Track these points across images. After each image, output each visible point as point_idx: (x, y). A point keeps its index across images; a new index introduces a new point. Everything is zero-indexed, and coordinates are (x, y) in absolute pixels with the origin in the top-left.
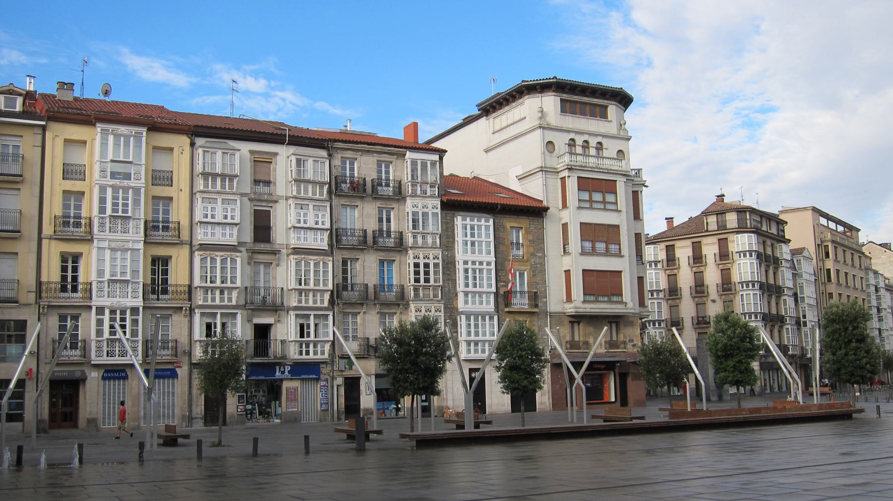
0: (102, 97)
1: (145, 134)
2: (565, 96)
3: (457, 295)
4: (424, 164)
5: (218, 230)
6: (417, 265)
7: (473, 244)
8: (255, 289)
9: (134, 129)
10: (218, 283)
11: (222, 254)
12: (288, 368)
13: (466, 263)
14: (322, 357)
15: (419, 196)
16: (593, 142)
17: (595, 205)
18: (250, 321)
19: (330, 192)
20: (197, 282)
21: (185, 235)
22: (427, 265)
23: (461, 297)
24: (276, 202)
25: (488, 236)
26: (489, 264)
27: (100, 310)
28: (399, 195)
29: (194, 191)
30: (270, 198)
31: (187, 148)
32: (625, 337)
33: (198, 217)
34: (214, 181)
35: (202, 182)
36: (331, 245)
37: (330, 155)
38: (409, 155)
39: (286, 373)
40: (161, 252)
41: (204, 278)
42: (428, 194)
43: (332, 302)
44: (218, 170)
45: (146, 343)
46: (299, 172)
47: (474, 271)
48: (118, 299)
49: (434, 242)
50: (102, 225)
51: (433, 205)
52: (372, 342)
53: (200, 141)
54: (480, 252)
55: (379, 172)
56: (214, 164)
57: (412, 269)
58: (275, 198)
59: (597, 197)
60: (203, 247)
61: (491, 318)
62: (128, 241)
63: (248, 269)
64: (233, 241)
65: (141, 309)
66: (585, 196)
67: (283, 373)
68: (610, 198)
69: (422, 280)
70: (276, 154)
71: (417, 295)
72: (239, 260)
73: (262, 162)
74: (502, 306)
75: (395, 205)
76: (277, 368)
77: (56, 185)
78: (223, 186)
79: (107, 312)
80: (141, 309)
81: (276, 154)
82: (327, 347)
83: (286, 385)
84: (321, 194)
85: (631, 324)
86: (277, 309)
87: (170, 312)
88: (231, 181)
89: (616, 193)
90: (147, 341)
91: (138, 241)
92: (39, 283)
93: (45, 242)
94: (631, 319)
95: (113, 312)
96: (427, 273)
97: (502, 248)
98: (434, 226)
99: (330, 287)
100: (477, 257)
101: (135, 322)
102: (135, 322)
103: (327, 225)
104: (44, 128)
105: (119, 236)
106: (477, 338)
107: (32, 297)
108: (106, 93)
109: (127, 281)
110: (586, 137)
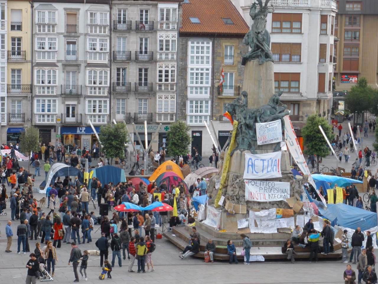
1: (6, 4)
3: (186, 88)
4: (168, 11)
6: (161, 71)
7: (197, 57)
8: (68, 86)
12: (84, 129)
13: (192, 69)
14: (103, 123)
15: (165, 30)
17: (284, 31)
18: (63, 103)
19: (110, 30)
20: (35, 83)
21: (29, 58)
22: (167, 72)
23: (189, 90)
24: (79, 37)
25: (208, 52)
26: (207, 69)
28: (153, 29)
29: (34, 33)
31: (30, 9)
32: (303, 113)
33: (36, 48)
34: (44, 27)
35: (37, 28)
36: (110, 61)
37: (111, 8)
39: (83, 131)
40: (17, 67)
42: (171, 28)
43: (110, 93)
44: (47, 21)
45: (9, 114)
46: (91, 20)
47: (197, 74)
49: (172, 58)
51: (172, 36)
52: (132, 115)
54: (202, 62)
55: (142, 15)
56: (44, 19)
57: (158, 74)
58: (78, 35)
59: (286, 25)
60: (39, 64)
61: (207, 102)
63: (63, 75)
65: (6, 98)
66: (278, 25)
67: (81, 131)
68: (296, 25)
69: (163, 80)
70: (79, 9)
71: (160, 89)
72: (57, 71)
73: (72, 14)
74: (216, 94)
75: (149, 35)
76: (78, 128)
78: (49, 31)
80: (6, 98)
81: (79, 9)
82: (106, 118)
83: (83, 137)
84: (105, 32)
85: (309, 105)
86: (78, 96)
87: (21, 99)
88: (53, 26)
89: (301, 22)
90: (9, 114)
94: (308, 102)
96: (167, 76)
97: (218, 59)
98: (174, 48)
99: (108, 85)
100: (200, 66)
103: (108, 50)
106: (197, 114)
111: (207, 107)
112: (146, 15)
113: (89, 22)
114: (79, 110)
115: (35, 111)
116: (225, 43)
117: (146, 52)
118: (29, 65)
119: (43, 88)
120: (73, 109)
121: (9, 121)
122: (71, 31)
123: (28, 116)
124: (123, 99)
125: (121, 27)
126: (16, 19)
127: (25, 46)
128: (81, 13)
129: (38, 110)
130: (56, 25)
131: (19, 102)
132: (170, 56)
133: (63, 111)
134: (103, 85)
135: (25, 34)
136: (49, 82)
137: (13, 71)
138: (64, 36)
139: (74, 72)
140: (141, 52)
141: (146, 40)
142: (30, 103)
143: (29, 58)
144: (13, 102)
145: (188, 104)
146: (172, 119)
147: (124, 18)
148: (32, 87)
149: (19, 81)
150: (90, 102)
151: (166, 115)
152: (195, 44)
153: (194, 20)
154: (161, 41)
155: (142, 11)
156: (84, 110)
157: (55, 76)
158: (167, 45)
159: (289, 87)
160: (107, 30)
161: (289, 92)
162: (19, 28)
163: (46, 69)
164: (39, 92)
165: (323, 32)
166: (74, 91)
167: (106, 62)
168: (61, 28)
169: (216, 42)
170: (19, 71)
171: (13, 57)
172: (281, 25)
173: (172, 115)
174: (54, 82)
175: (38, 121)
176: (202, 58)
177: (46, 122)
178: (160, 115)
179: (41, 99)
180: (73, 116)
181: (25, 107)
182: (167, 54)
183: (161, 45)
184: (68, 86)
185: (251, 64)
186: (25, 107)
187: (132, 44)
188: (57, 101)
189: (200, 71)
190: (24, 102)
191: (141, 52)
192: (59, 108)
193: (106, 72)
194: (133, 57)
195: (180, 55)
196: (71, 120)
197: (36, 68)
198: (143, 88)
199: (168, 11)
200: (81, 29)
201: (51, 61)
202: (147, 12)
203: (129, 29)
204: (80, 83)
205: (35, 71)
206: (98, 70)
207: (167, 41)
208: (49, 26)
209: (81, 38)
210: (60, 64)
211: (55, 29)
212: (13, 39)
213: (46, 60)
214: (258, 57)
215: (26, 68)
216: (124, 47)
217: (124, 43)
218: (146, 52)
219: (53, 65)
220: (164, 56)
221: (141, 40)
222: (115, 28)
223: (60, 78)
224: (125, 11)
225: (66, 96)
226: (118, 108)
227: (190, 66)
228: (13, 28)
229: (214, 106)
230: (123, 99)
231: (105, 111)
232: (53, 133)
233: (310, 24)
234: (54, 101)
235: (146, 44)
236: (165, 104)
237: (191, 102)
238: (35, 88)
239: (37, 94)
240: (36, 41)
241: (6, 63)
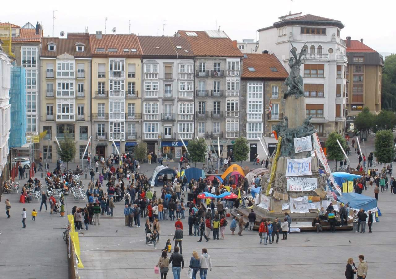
0: (113, 33)
2: (303, 26)
3: (246, 115)
4: (233, 63)
6: (228, 104)
7: (254, 94)
9: (121, 59)
11: (152, 102)
12: (177, 143)
13: (250, 102)
14: (190, 139)
15: (231, 76)
16: (316, 46)
17: (312, 76)
18: (163, 125)
19: (194, 76)
20: (144, 112)
21: (140, 96)
22: (233, 104)
23: (248, 116)
24: (173, 81)
25: (261, 91)
26: (260, 102)
27: (111, 123)
28: (223, 76)
29: (143, 79)
30: (171, 80)
31: (140, 63)
32: (326, 131)
33: (145, 89)
37: (195, 62)
38: (228, 60)
39: (176, 144)
40: (131, 102)
42: (235, 75)
43: (194, 118)
44: (152, 72)
45: (126, 133)
46: (181, 70)
47: (253, 105)
48: (117, 119)
49: (237, 95)
50: (111, 94)
51: (237, 80)
52: (210, 134)
53: (145, 60)
55: (215, 66)
56: (150, 70)
57: (227, 105)
58: (173, 80)
59: (313, 72)
60: (146, 100)
61: (260, 124)
62: (120, 99)
63: (162, 107)
65: (125, 123)
66: (308, 72)
67: (175, 144)
68: (320, 72)
69: (231, 109)
70: (173, 63)
71: (228, 115)
72: (159, 104)
73: (168, 66)
74: (266, 119)
75: (221, 79)
76: (173, 142)
78: (153, 77)
79: (114, 124)
80: (125, 123)
81: (173, 63)
82: (192, 136)
83: (176, 149)
84: (190, 78)
85: (330, 126)
86: (173, 121)
88: (156, 74)
89: (324, 70)
90: (127, 133)
91: (124, 99)
92: (91, 114)
93: (93, 100)
94: (329, 124)
95: (115, 124)
96: (233, 107)
97: (268, 95)
98: (237, 88)
99: (193, 113)
100: (255, 100)
101: (123, 127)
102: (123, 127)
103: (193, 90)
104: (91, 61)
105: (117, 97)
106: (253, 132)
107: (89, 119)
108: (114, 31)
109: (120, 113)
110: (313, 44)
111: (260, 127)
112: (219, 66)
113: (180, 71)
114: (174, 130)
115: (144, 131)
116: (272, 84)
117: (218, 91)
118: (140, 100)
119: (150, 115)
120: (170, 129)
121: (126, 138)
122: (168, 78)
123: (139, 134)
124: (203, 123)
125: (201, 74)
126: (131, 70)
127: (137, 88)
128: (175, 65)
129: (146, 130)
130: (158, 73)
131: (134, 125)
132: (235, 94)
133: (163, 131)
134: (190, 113)
135: (137, 80)
136: (154, 112)
137: (129, 104)
138: (164, 81)
139: (170, 105)
140: (215, 91)
141: (218, 83)
143: (140, 96)
144: (130, 125)
145: (248, 125)
146: (236, 136)
147: (204, 68)
148: (142, 115)
149: (133, 111)
150: (181, 124)
151: (232, 133)
152: (252, 85)
153: (251, 69)
154: (229, 83)
155: (215, 64)
156: (177, 130)
157: (157, 108)
158: (233, 86)
159: (316, 114)
160: (192, 76)
161: (316, 117)
162: (134, 76)
164: (147, 118)
165: (339, 76)
166: (170, 118)
167: (192, 98)
168: (161, 75)
169: (266, 84)
170: (133, 104)
171: (129, 95)
172: (310, 72)
173: (236, 133)
174: (157, 111)
175: (146, 138)
176: (257, 94)
177: (151, 138)
178: (228, 133)
180: (170, 134)
181: (137, 128)
182: (233, 92)
183: (229, 86)
185: (291, 98)
186: (137, 129)
187: (209, 85)
188: (159, 124)
189: (255, 103)
190: (137, 125)
191: (215, 91)
192: (160, 129)
193: (191, 105)
194: (210, 94)
195: (242, 92)
196: (168, 137)
198: (217, 115)
199: (233, 63)
200: (175, 76)
201: (155, 97)
202: (219, 64)
203: (207, 76)
204: (174, 112)
206: (186, 103)
207: (233, 83)
208: (153, 74)
209: (175, 81)
210: (160, 100)
211: (158, 76)
212: (130, 83)
213: (152, 97)
214: (294, 93)
215: (138, 103)
216: (204, 88)
217: (204, 85)
218: (218, 91)
219: (156, 100)
220: (230, 94)
221: (215, 82)
222: (198, 75)
223: (160, 108)
224: (204, 64)
225: (165, 121)
226: (200, 129)
227: (248, 100)
228: (129, 76)
229: (265, 127)
230: (203, 123)
231: (191, 131)
232: (156, 146)
233: (330, 71)
234: (157, 124)
235: (218, 86)
236: (232, 126)
237: (250, 124)
238: (144, 116)
239: (145, 120)
240: (145, 84)
241: (125, 100)
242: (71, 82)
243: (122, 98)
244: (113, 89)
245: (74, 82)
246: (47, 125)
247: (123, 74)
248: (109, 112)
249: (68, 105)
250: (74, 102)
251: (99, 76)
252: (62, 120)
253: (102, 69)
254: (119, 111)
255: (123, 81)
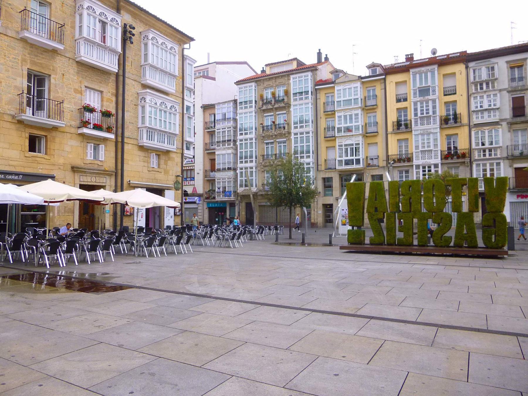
0: (433, 56)
1: (436, 68)
5: (486, 114)
8: (516, 147)
9: (430, 68)
10: (487, 145)
11: (488, 128)
20: (474, 146)
21: (465, 120)
27: (418, 167)
29: (470, 93)
30: (523, 88)
33: (473, 108)
34: (481, 84)
35: (473, 88)
41: (477, 144)
48: (427, 160)
50: (416, 122)
56: (480, 76)
62: (431, 129)
63: (508, 135)
64: (496, 119)
77: (393, 106)
79: (421, 167)
87: (458, 165)
88: (493, 83)
91: (436, 128)
92: (388, 156)
93: (389, 136)
95: (424, 167)
104: (385, 79)
105: (426, 127)
107: (384, 164)
108: (434, 53)
109: (431, 150)
118: (466, 129)
126: (449, 83)
127: (461, 109)
130: (496, 79)
136: (491, 143)
138: (508, 92)
142: (468, 169)
163: (486, 129)
164: (479, 156)
179: (481, 163)
184: (516, 147)
188: (502, 164)
197: (473, 129)
205: (473, 133)
210: (504, 124)
211: (496, 84)
219: (496, 123)
234: (498, 164)
238: (474, 152)
239: (476, 158)
241: (439, 129)
242: (356, 112)
243: (435, 126)
244: (419, 115)
245: (359, 112)
246: (327, 175)
247: (434, 91)
248: (414, 151)
249: (353, 145)
250: (360, 140)
251: (398, 101)
252: (344, 167)
253: (402, 90)
254: (429, 146)
255: (434, 101)
